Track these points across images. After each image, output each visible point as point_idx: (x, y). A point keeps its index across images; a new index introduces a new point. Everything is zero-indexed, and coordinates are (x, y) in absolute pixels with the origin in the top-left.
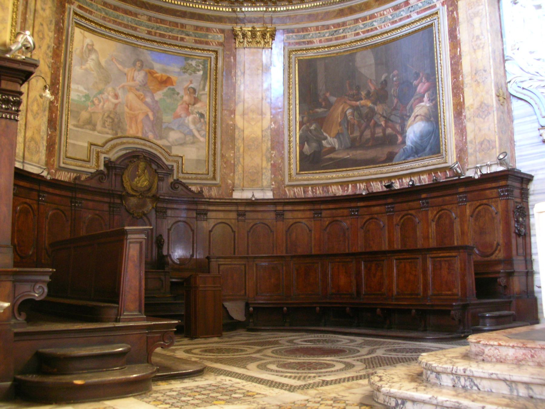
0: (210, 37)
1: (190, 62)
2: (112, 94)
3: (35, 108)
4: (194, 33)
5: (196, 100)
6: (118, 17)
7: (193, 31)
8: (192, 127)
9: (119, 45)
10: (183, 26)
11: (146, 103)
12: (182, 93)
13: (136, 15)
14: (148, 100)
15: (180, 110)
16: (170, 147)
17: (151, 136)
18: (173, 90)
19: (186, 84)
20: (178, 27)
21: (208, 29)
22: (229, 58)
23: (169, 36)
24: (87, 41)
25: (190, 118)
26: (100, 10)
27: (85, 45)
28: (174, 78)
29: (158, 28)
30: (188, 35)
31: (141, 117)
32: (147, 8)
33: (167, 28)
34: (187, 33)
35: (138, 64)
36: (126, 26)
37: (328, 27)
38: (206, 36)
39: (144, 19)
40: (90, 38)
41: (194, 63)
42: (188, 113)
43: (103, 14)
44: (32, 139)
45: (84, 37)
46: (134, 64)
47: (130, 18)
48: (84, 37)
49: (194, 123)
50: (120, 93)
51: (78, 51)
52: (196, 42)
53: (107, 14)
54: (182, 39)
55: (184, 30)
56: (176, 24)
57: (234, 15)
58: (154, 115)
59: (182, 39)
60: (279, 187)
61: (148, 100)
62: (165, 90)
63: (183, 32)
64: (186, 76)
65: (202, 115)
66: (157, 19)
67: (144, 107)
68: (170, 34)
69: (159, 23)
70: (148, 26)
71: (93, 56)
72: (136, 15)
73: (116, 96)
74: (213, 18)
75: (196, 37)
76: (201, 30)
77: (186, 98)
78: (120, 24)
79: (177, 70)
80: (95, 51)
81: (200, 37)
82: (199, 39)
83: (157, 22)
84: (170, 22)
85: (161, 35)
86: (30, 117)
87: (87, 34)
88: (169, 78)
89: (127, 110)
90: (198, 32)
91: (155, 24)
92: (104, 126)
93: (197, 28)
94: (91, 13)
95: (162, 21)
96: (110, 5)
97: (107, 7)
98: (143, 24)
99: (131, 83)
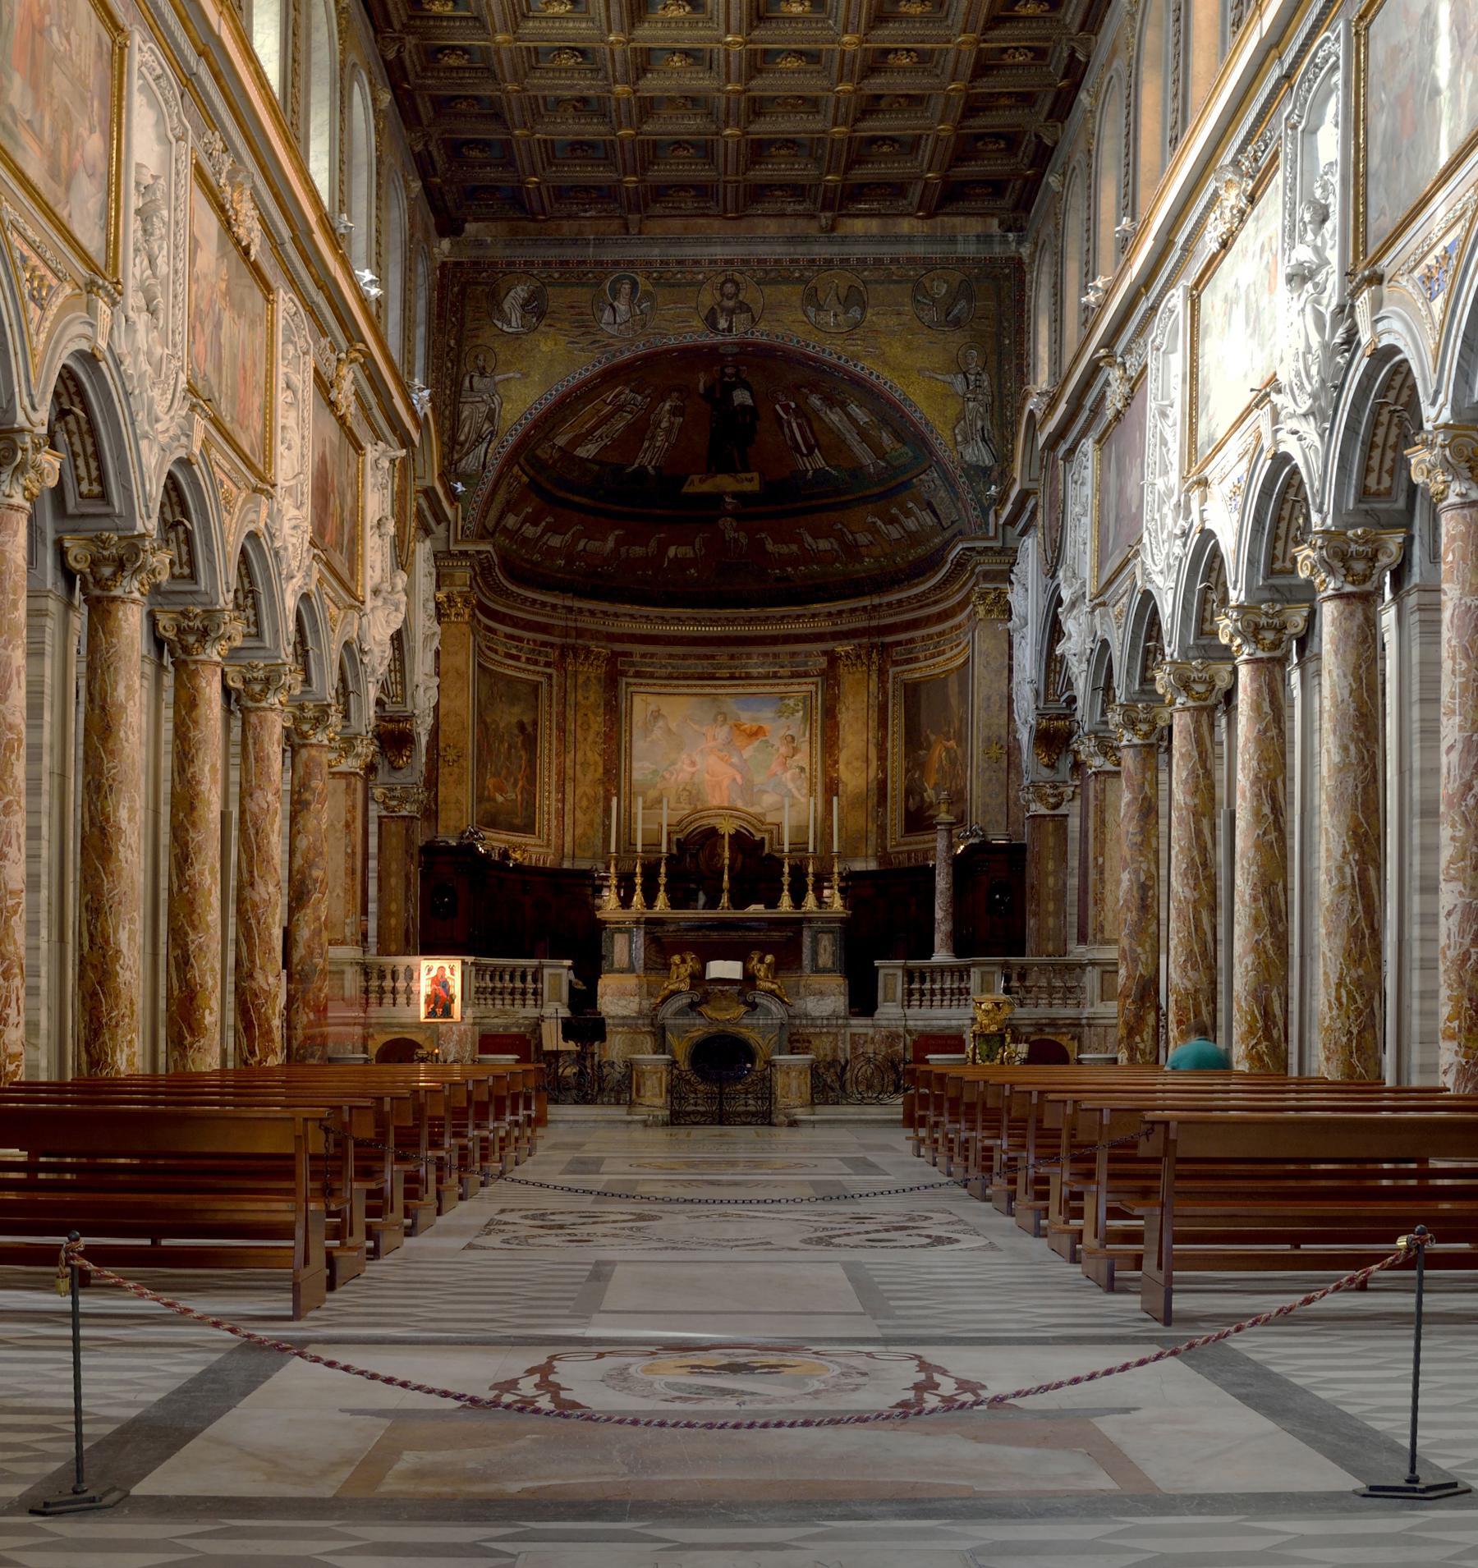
2: (687, 762)
3: (585, 803)
5: (795, 751)
8: (791, 785)
10: (776, 656)
11: (732, 765)
12: (777, 743)
13: (713, 657)
14: (735, 760)
15: (775, 767)
16: (764, 815)
17: (740, 804)
18: (767, 742)
19: (783, 732)
24: (652, 707)
25: (788, 774)
26: (665, 666)
28: (766, 726)
31: (726, 783)
32: (726, 645)
35: (720, 718)
37: (930, 637)
38: (806, 664)
41: (791, 702)
42: (786, 769)
43: (670, 670)
44: (584, 834)
46: (715, 720)
47: (705, 662)
48: (647, 704)
49: (793, 780)
50: (698, 759)
57: (837, 628)
58: (743, 777)
60: (883, 857)
61: (735, 760)
62: (756, 743)
64: (783, 719)
65: (802, 769)
67: (731, 771)
71: (661, 723)
72: (713, 657)
73: (693, 764)
77: (783, 750)
79: (771, 715)
86: (579, 814)
87: (651, 698)
88: (760, 728)
89: (707, 777)
92: (678, 801)
93: (793, 654)
99: (712, 744)
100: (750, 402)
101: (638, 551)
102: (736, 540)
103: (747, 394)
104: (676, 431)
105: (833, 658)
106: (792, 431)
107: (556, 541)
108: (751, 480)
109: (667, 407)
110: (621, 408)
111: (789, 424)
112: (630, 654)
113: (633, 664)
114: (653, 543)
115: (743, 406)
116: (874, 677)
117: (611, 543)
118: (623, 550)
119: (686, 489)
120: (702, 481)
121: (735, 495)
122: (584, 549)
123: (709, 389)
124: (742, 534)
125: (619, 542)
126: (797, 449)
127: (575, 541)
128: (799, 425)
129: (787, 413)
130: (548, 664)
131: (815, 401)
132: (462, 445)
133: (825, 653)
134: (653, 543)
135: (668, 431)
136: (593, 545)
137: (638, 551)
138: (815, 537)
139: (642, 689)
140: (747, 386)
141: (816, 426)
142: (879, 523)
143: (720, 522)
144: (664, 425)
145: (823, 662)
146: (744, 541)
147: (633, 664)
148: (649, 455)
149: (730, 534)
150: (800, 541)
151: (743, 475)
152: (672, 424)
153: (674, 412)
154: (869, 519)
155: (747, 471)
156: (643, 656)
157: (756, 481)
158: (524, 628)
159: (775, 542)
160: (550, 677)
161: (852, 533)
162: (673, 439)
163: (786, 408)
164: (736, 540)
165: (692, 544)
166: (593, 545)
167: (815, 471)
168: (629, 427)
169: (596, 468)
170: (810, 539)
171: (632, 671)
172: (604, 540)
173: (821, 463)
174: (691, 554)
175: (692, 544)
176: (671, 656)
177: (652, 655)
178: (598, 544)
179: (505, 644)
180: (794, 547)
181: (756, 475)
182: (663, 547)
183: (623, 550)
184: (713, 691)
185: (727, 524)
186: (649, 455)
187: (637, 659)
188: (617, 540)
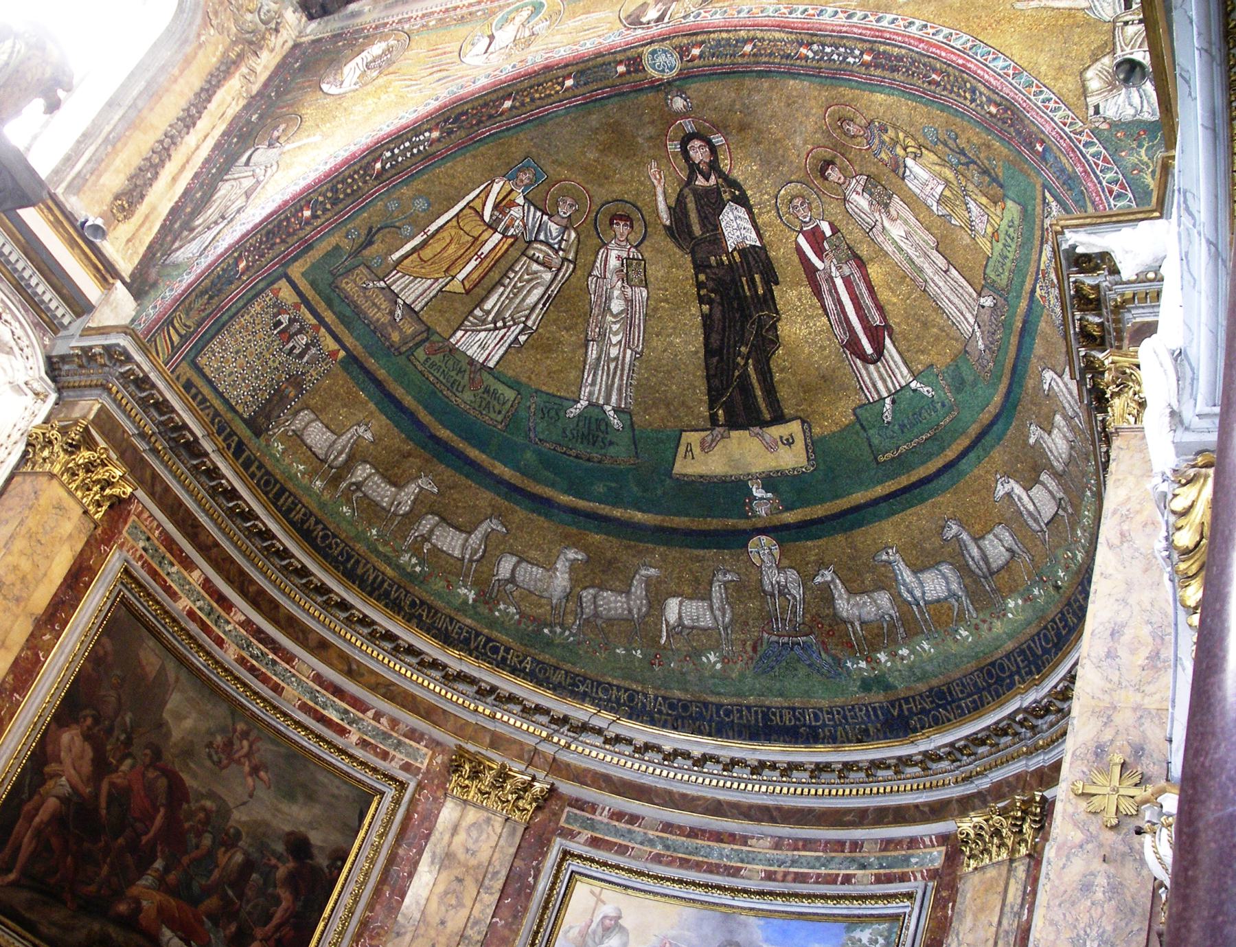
0: (913, 860)
1: (857, 934)
4: (878, 858)
6: (696, 851)
7: (878, 854)
9: (689, 912)
10: (856, 845)
13: (744, 840)
20: (843, 851)
21: (913, 842)
22: (945, 907)
23: (819, 876)
24: (608, 910)
26: (651, 843)
27: (597, 919)
29: (794, 862)
30: (863, 867)
32: (773, 820)
33: (818, 858)
34: (862, 861)
36: (712, 869)
38: (906, 860)
39: (762, 847)
40: (613, 901)
43: (659, 849)
45: (600, 901)
47: (727, 848)
48: (600, 901)
51: (574, 933)
52: (879, 880)
53: (667, 847)
54: (847, 879)
55: (857, 854)
56: (840, 844)
59: (847, 879)
63: (853, 860)
66: (796, 840)
68: (823, 871)
69: (798, 850)
70: (770, 862)
72: (744, 840)
74: (926, 809)
75: (881, 867)
76: (896, 849)
78: (698, 866)
80: (622, 929)
81: (889, 867)
82: (888, 871)
83: (796, 849)
84: (827, 842)
85: (801, 878)
87: (609, 894)
90: (888, 854)
91: (790, 853)
93: (888, 844)
94: (623, 850)
95: (808, 844)
96: (680, 827)
97: (671, 833)
98: (760, 856)
100: (752, 239)
101: (612, 603)
102: (783, 591)
103: (742, 212)
104: (638, 319)
105: (954, 847)
106: (839, 302)
107: (451, 542)
108: (790, 442)
109: (613, 263)
110: (522, 245)
111: (830, 280)
112: (593, 808)
113: (592, 826)
114: (638, 589)
115: (745, 252)
116: (1021, 870)
117: (561, 580)
118: (587, 595)
119: (685, 467)
120: (706, 447)
121: (770, 481)
122: (512, 579)
123: (678, 210)
124: (792, 575)
125: (580, 577)
126: (853, 346)
127: (490, 555)
128: (847, 282)
129: (820, 253)
130: (406, 767)
131: (861, 201)
132: (192, 230)
133: (944, 839)
134: (638, 589)
135: (627, 319)
136: (530, 574)
137: (612, 603)
138: (916, 570)
139: (595, 870)
140: (743, 201)
141: (874, 271)
142: (1018, 490)
143: (752, 546)
144: (617, 306)
145: (937, 856)
146: (797, 592)
147: (592, 826)
148: (602, 378)
149: (772, 578)
150: (886, 582)
151: (776, 431)
152: (629, 302)
153: (632, 271)
154: (1001, 491)
155: (779, 418)
156: (618, 815)
157: (800, 443)
158: (374, 688)
159: (851, 592)
160: (402, 786)
161: (977, 539)
162: (638, 335)
163: (815, 238)
164: (783, 591)
165: (707, 597)
166: (530, 574)
167: (896, 396)
168: (548, 300)
169: (510, 394)
170: (907, 575)
171: (587, 834)
172: (550, 567)
173: (903, 375)
174: (707, 621)
175: (707, 597)
176: (668, 827)
177: (633, 819)
178: (538, 572)
179: (312, 693)
180: (884, 599)
181: (795, 427)
182: (656, 602)
183: (587, 595)
184: (726, 899)
185: (762, 548)
186: (602, 378)
187: (602, 818)
188: (573, 567)
